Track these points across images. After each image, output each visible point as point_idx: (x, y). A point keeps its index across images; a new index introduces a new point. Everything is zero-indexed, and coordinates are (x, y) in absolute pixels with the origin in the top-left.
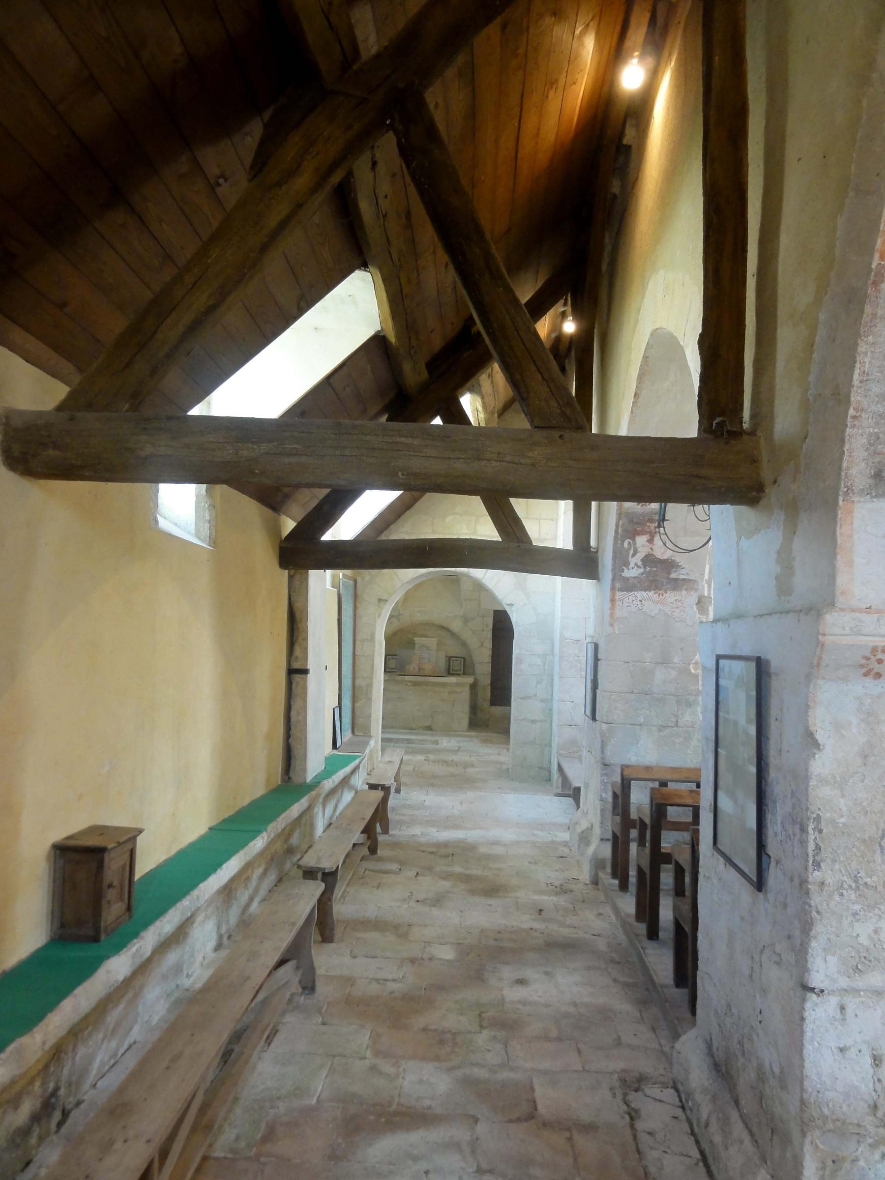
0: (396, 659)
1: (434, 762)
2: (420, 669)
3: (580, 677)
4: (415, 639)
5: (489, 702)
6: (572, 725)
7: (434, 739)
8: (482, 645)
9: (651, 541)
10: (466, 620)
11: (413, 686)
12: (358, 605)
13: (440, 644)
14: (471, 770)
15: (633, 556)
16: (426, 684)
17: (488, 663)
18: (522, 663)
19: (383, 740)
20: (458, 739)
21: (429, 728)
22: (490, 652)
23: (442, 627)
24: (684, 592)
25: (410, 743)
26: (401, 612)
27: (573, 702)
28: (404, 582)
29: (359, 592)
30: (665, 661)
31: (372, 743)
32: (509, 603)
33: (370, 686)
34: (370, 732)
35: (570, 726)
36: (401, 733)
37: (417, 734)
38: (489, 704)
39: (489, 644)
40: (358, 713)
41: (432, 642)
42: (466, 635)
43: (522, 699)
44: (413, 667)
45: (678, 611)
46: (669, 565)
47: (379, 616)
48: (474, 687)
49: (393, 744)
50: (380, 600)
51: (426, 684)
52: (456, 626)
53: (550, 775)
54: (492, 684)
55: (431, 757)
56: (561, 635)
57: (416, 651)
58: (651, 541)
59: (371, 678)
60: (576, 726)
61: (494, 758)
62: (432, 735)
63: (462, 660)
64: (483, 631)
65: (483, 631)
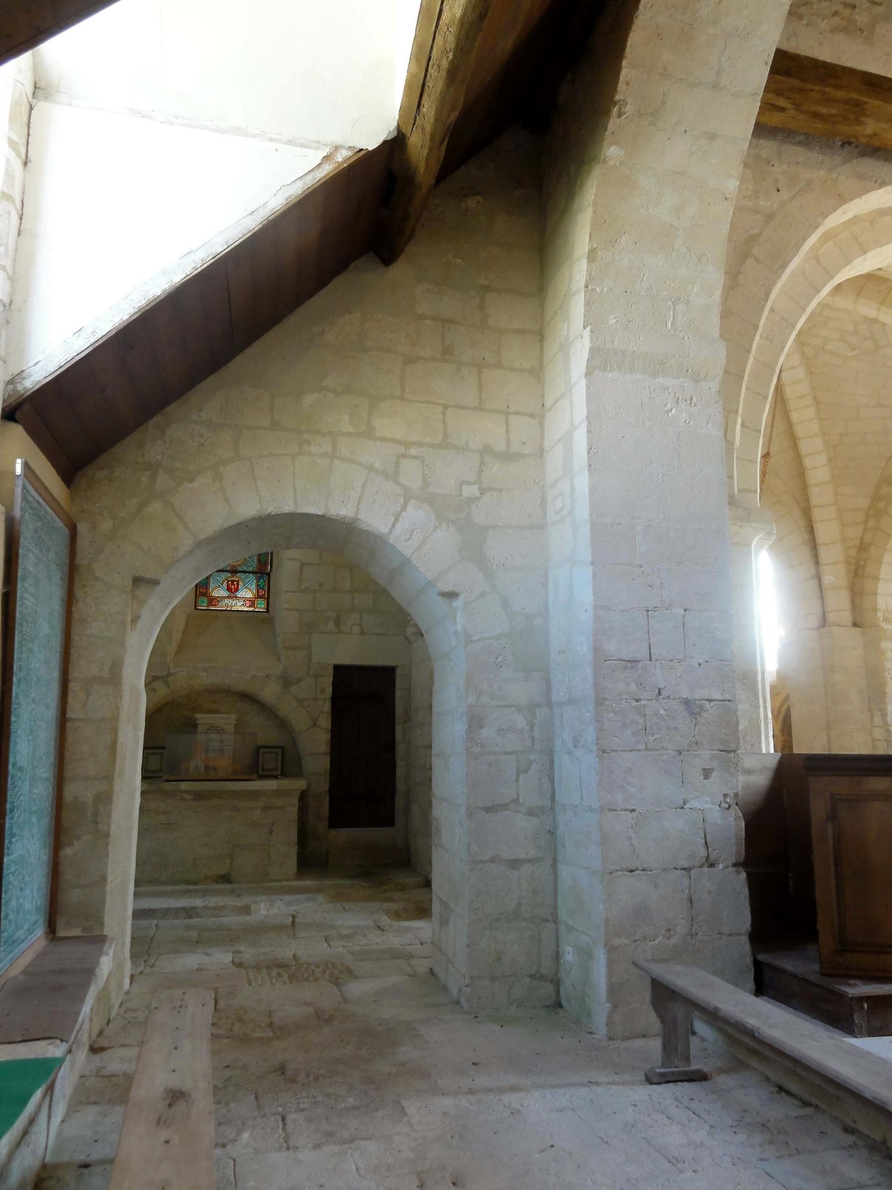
0: (161, 754)
1: (257, 968)
2: (207, 768)
3: (646, 749)
4: (198, 716)
5: (326, 823)
6: (637, 869)
7: (238, 902)
8: (315, 725)
10: (287, 682)
11: (195, 799)
12: (79, 592)
13: (240, 725)
14: (355, 989)
16: (219, 794)
17: (326, 754)
18: (481, 727)
19: (138, 914)
20: (289, 898)
21: (226, 879)
22: (329, 736)
23: (246, 697)
25: (190, 917)
26: (172, 671)
27: (633, 810)
28: (202, 536)
29: (82, 560)
31: (106, 964)
32: (448, 588)
33: (105, 799)
34: (102, 924)
35: (632, 871)
36: (172, 894)
37: (205, 893)
38: (327, 825)
39: (325, 722)
40: (68, 874)
41: (226, 720)
42: (288, 709)
43: (488, 810)
44: (196, 763)
47: (135, 620)
48: (303, 796)
49: (155, 922)
50: (137, 581)
51: (219, 794)
52: (269, 693)
53: (558, 993)
54: (331, 791)
55: (248, 953)
56: (597, 650)
57: (198, 737)
59: (109, 777)
60: (644, 870)
61: (375, 940)
62: (232, 892)
63: (280, 751)
64: (316, 699)
65: (316, 699)
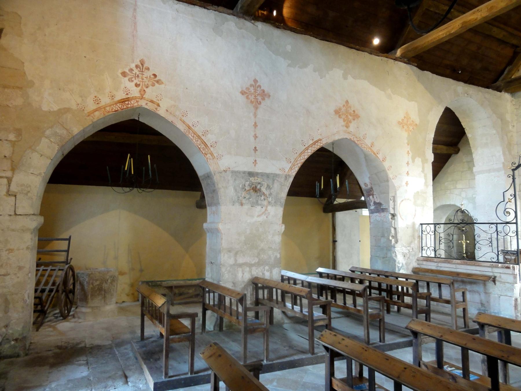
9: (373, 197)
15: (371, 202)
24: (385, 213)
30: (383, 236)
45: (385, 219)
46: (380, 204)
58: (373, 197)
